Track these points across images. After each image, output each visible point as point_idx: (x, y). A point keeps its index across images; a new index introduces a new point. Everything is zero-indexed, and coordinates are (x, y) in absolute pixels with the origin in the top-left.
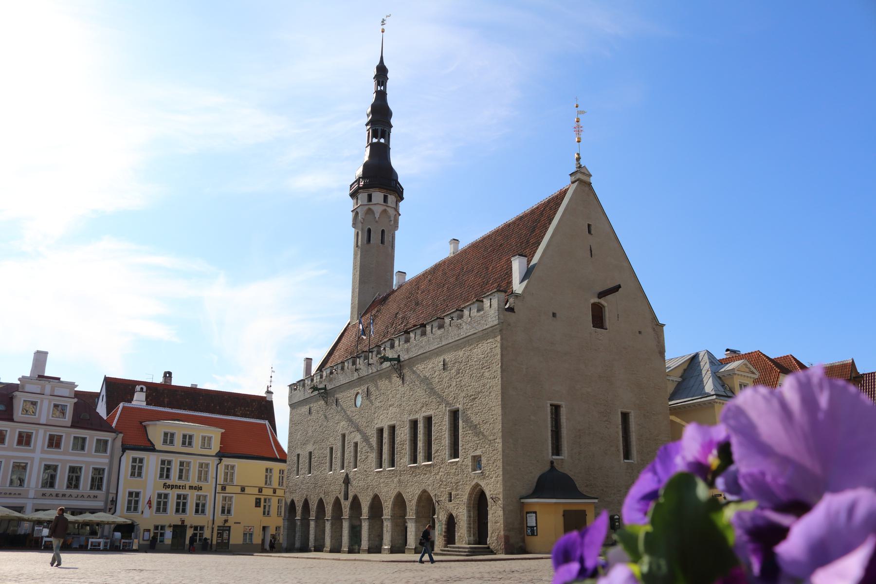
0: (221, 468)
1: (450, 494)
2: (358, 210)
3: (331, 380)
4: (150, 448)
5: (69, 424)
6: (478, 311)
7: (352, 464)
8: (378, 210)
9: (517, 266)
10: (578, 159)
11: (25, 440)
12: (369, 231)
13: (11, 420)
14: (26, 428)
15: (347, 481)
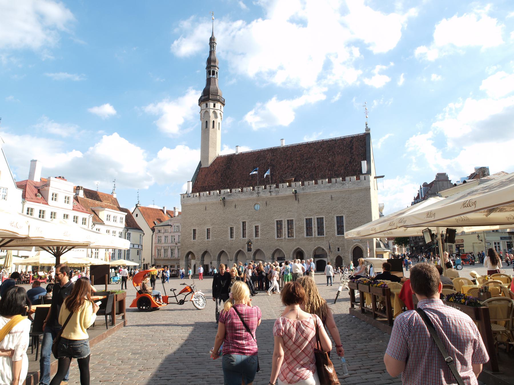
0: (127, 233)
1: (339, 249)
2: (208, 110)
3: (229, 195)
4: (102, 223)
5: (72, 208)
6: (357, 179)
7: (254, 235)
8: (218, 112)
9: (364, 164)
10: (366, 124)
11: (53, 215)
12: (214, 121)
13: (47, 204)
14: (54, 211)
15: (249, 243)
